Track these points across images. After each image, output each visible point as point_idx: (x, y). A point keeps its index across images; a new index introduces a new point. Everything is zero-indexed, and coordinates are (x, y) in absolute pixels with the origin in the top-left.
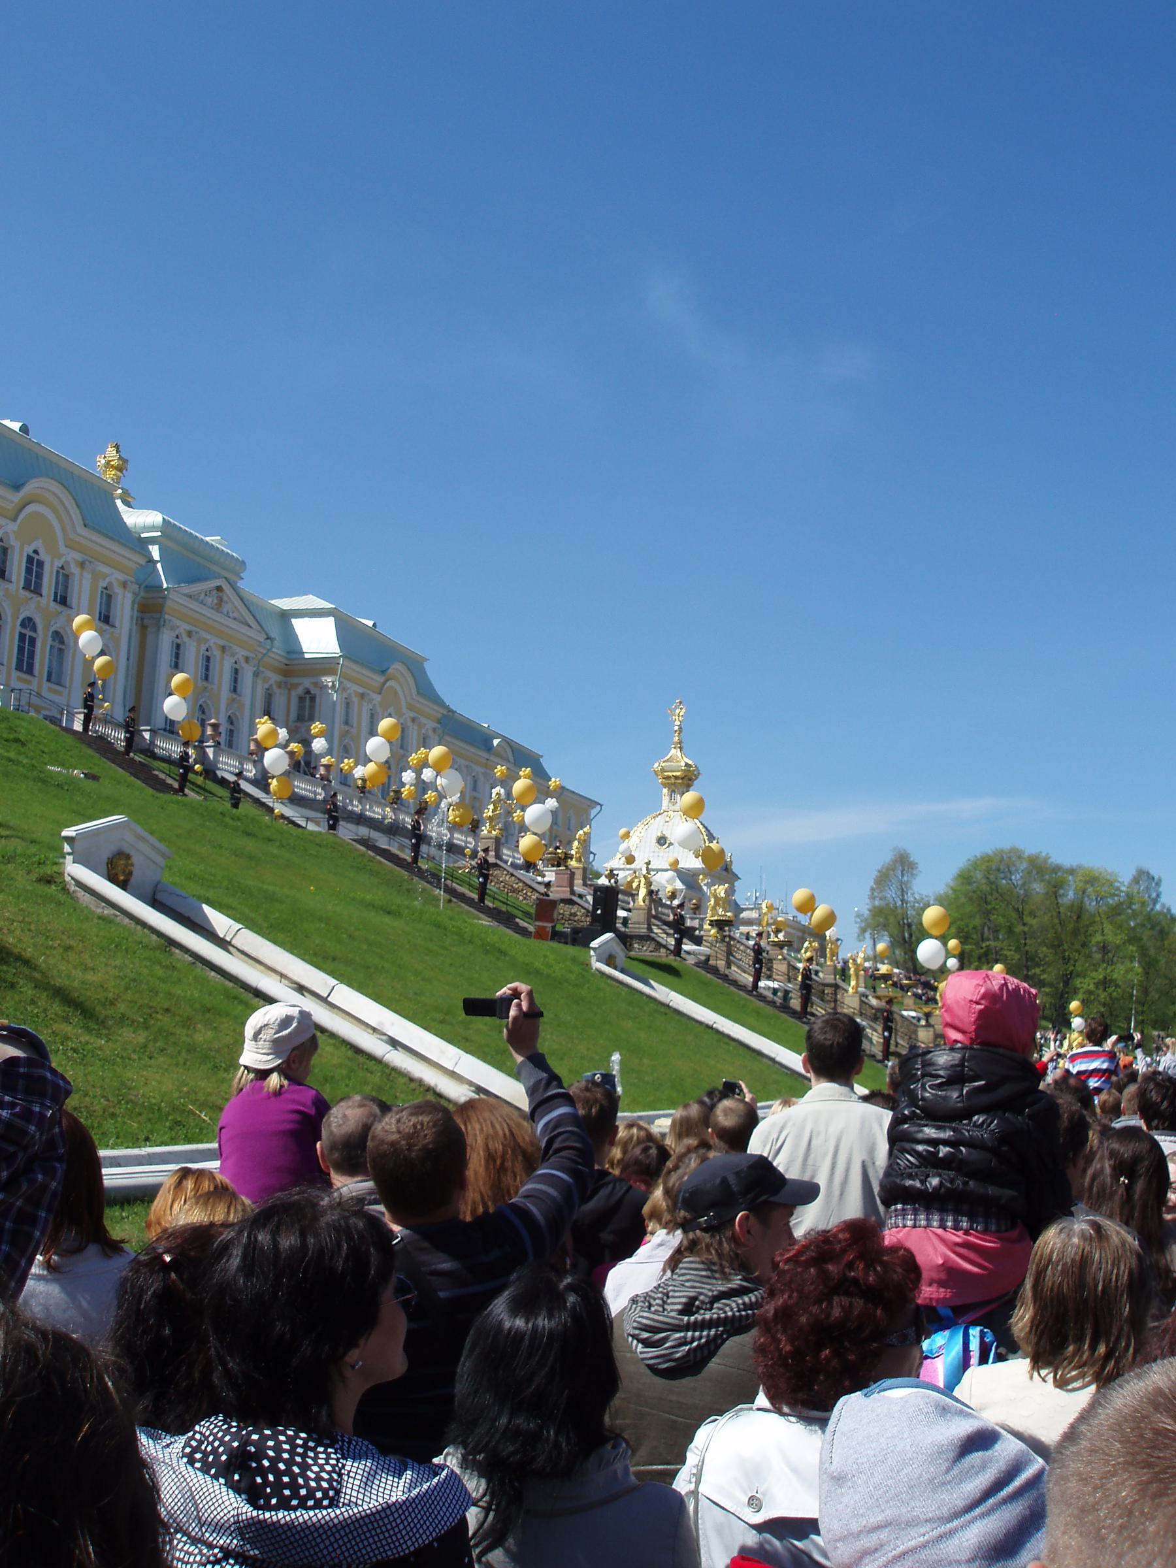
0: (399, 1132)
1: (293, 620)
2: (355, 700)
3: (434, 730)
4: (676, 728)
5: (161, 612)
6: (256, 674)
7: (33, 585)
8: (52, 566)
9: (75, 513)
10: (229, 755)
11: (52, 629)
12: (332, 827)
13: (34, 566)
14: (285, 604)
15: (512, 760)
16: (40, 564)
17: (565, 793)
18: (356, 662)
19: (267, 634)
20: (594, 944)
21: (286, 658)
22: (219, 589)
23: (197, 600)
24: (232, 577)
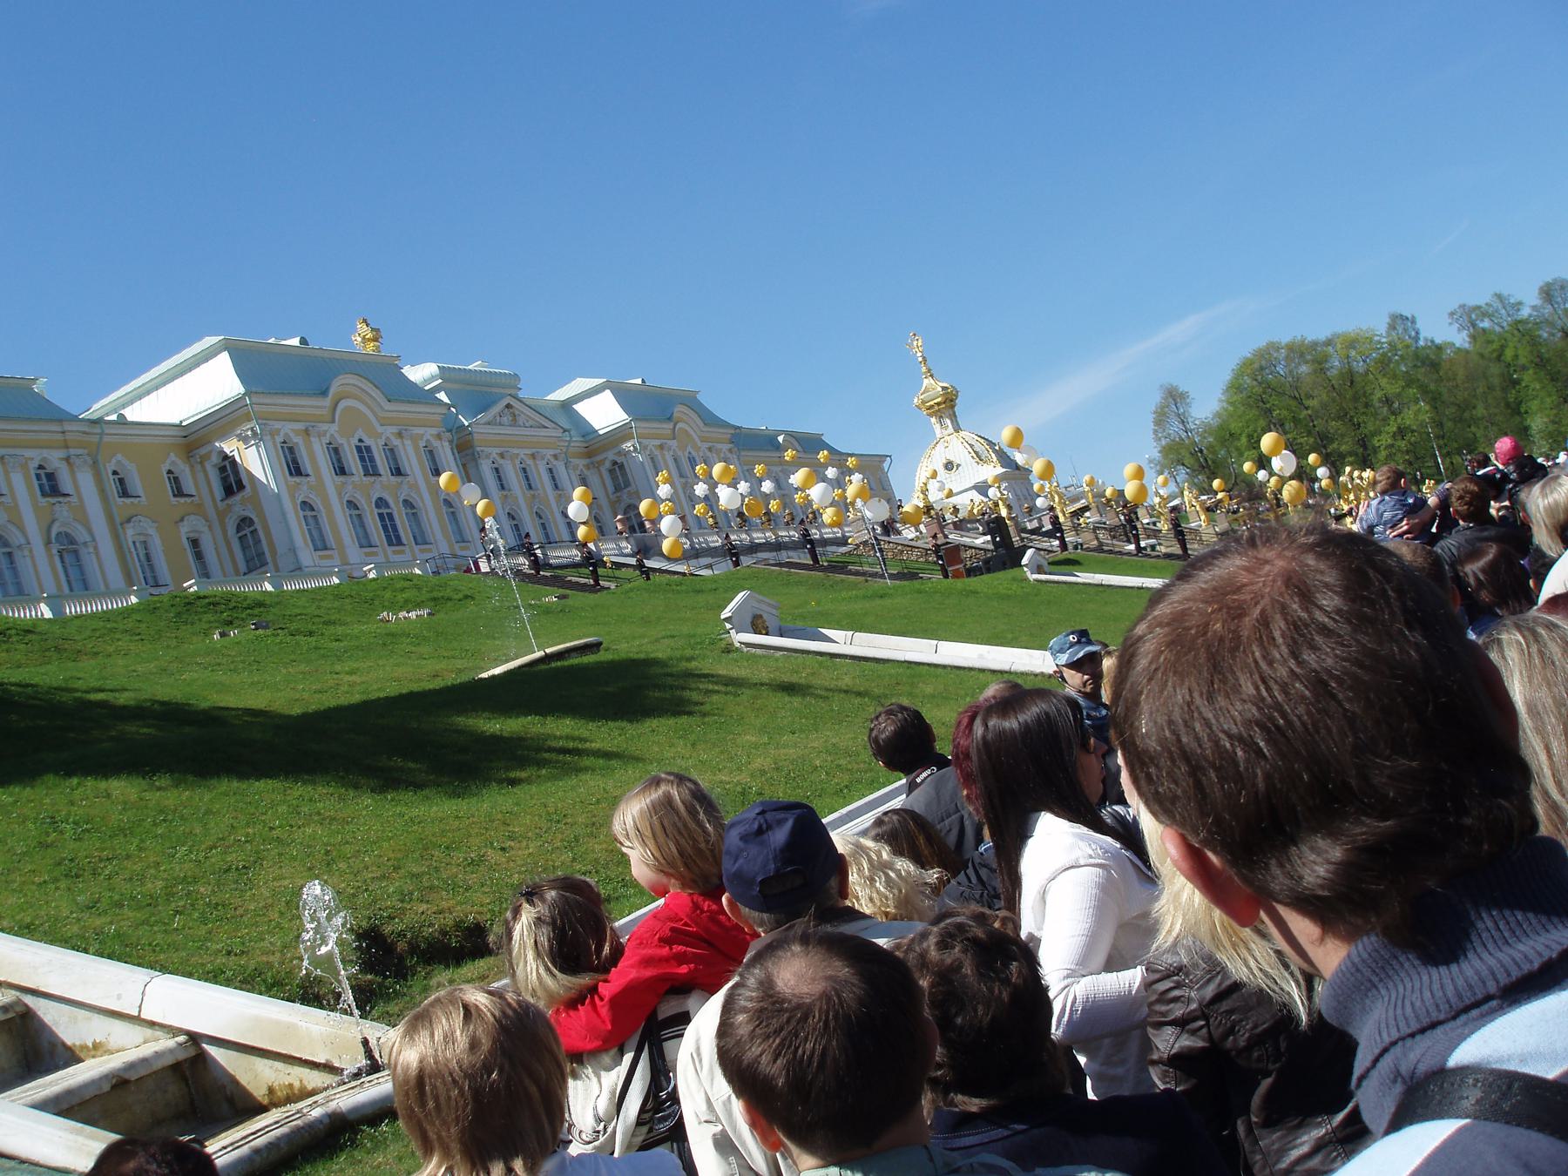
1: (574, 406)
2: (657, 452)
3: (730, 451)
4: (920, 359)
5: (472, 447)
7: (371, 470)
8: (349, 445)
9: (375, 393)
10: (605, 541)
11: (401, 500)
12: (737, 564)
13: (364, 452)
16: (368, 449)
18: (646, 420)
20: (1025, 561)
21: (586, 442)
22: (508, 406)
23: (495, 425)
24: (513, 392)
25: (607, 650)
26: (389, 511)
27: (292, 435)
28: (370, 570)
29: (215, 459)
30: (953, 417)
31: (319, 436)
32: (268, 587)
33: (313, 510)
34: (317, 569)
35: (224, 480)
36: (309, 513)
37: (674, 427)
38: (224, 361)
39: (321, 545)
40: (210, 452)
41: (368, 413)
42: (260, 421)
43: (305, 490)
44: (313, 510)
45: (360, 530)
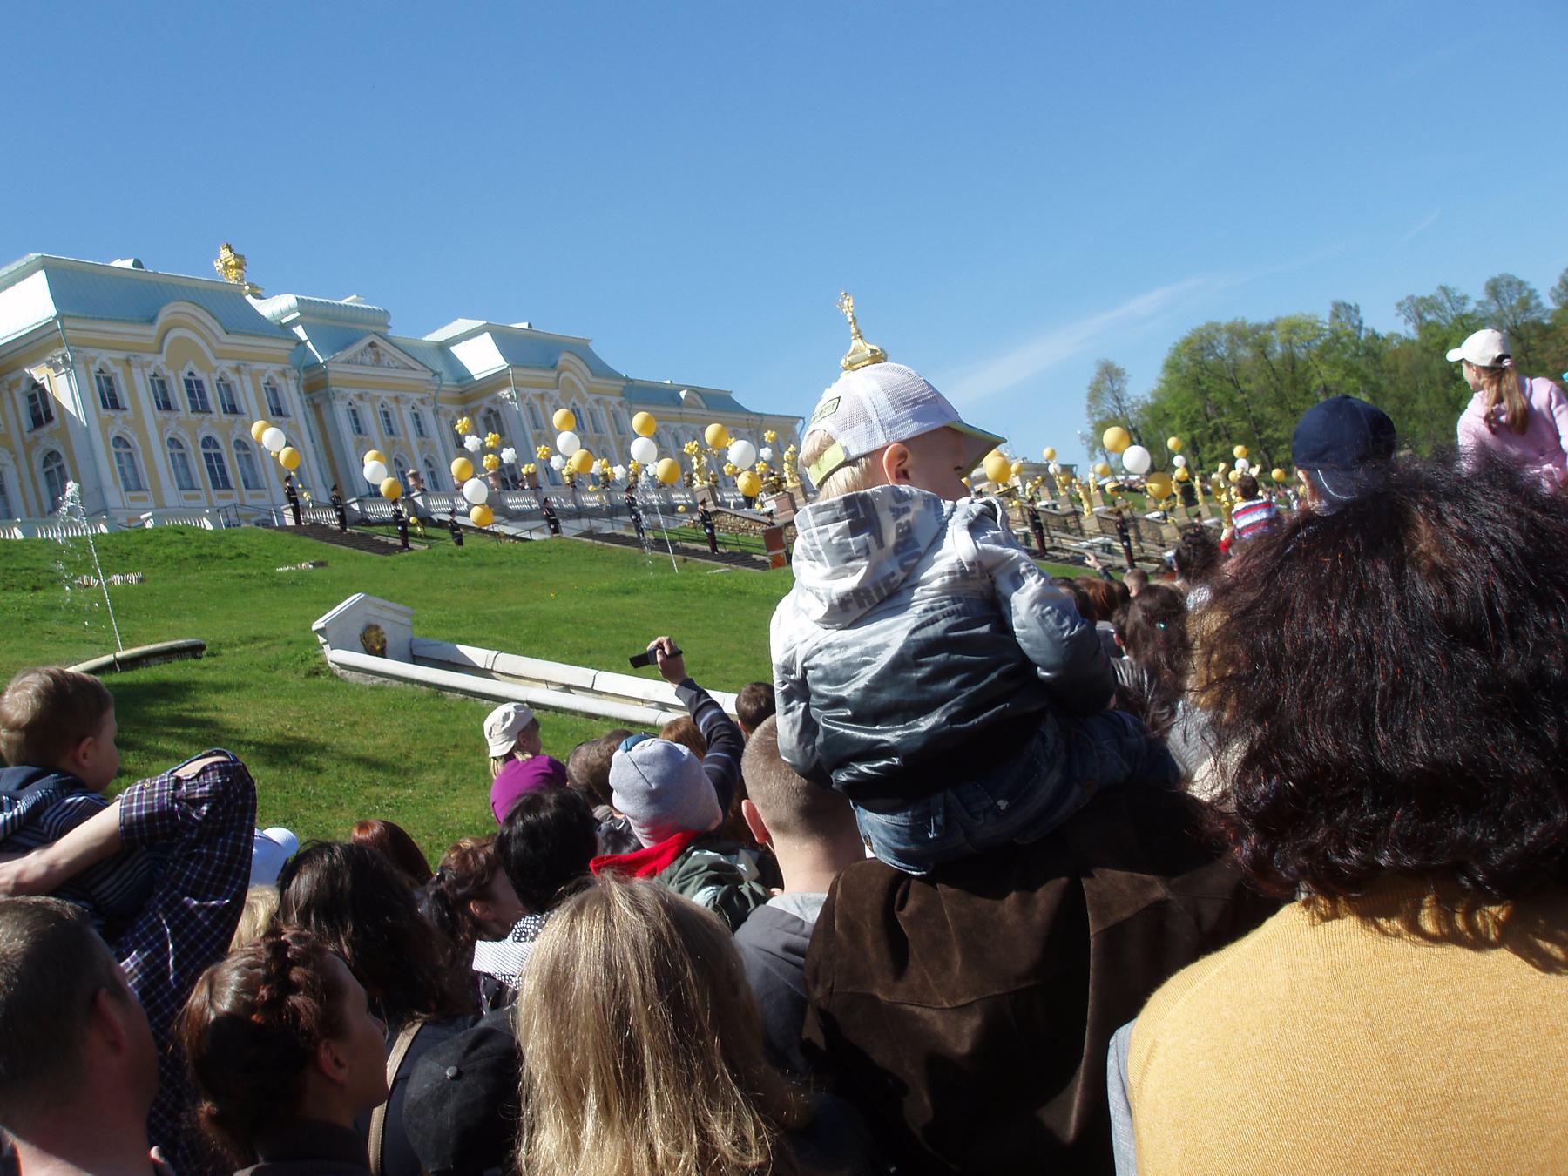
0: (601, 757)
1: (452, 349)
2: (537, 403)
3: (621, 404)
4: (850, 319)
6: (436, 412)
7: (199, 404)
8: (210, 380)
10: (437, 497)
12: (556, 531)
13: (194, 388)
14: (438, 336)
15: (703, 405)
16: (199, 384)
17: (765, 418)
18: (526, 367)
19: (432, 371)
21: (460, 387)
22: (372, 345)
25: (211, 655)
26: (216, 451)
27: (109, 363)
29: (24, 387)
31: (142, 368)
32: (18, 534)
34: (181, 509)
35: (34, 409)
36: (123, 450)
37: (558, 377)
38: (40, 278)
39: (133, 484)
40: (19, 379)
42: (72, 348)
43: (119, 423)
44: (128, 446)
45: (182, 471)
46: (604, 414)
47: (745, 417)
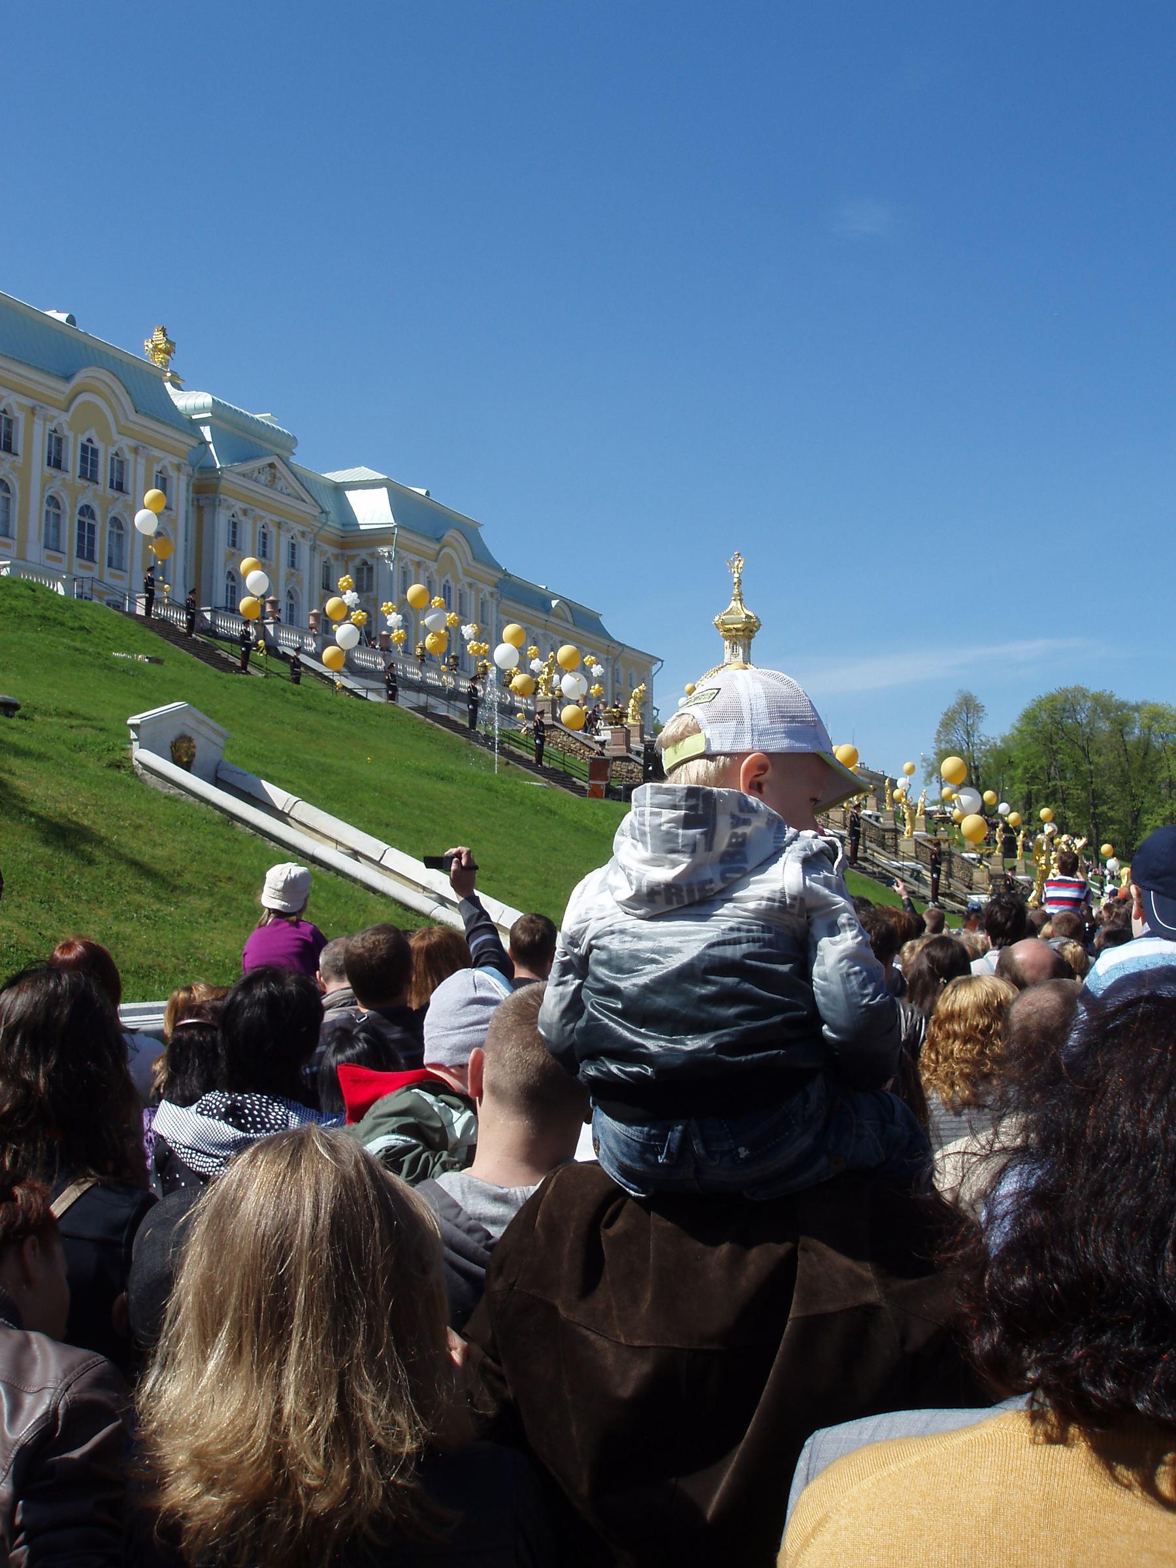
0: (363, 947)
1: (346, 492)
2: (412, 568)
3: (492, 594)
4: (736, 580)
6: (313, 548)
7: (89, 472)
8: (106, 451)
10: (289, 631)
11: (110, 516)
12: (392, 697)
13: (89, 454)
15: (570, 619)
16: (95, 452)
22: (272, 466)
23: (250, 478)
24: (284, 454)
27: (15, 407)
28: (5, 566)
30: (747, 648)
31: (45, 420)
33: (59, 508)
37: (440, 550)
41: (111, 420)
46: (473, 599)
47: (607, 642)
